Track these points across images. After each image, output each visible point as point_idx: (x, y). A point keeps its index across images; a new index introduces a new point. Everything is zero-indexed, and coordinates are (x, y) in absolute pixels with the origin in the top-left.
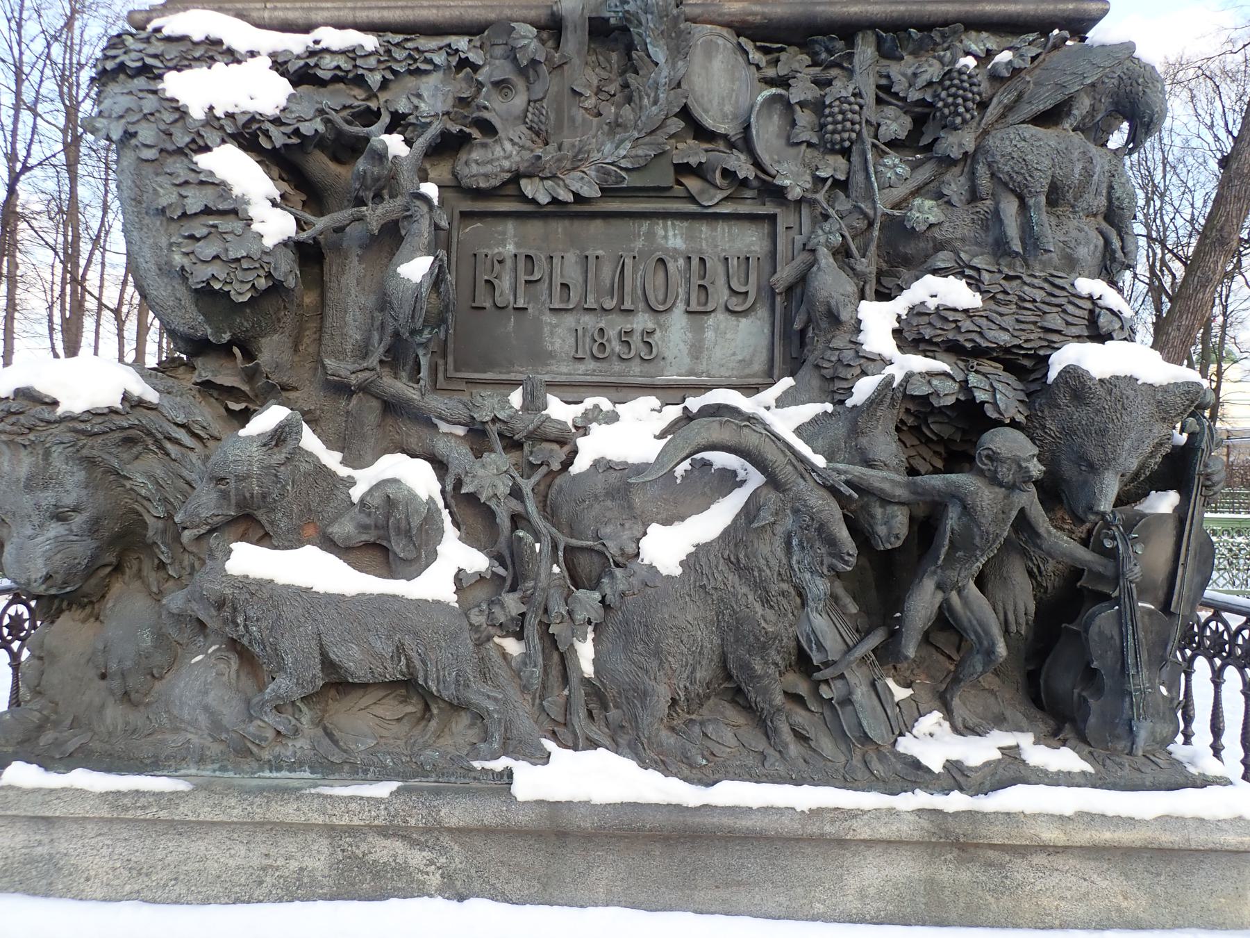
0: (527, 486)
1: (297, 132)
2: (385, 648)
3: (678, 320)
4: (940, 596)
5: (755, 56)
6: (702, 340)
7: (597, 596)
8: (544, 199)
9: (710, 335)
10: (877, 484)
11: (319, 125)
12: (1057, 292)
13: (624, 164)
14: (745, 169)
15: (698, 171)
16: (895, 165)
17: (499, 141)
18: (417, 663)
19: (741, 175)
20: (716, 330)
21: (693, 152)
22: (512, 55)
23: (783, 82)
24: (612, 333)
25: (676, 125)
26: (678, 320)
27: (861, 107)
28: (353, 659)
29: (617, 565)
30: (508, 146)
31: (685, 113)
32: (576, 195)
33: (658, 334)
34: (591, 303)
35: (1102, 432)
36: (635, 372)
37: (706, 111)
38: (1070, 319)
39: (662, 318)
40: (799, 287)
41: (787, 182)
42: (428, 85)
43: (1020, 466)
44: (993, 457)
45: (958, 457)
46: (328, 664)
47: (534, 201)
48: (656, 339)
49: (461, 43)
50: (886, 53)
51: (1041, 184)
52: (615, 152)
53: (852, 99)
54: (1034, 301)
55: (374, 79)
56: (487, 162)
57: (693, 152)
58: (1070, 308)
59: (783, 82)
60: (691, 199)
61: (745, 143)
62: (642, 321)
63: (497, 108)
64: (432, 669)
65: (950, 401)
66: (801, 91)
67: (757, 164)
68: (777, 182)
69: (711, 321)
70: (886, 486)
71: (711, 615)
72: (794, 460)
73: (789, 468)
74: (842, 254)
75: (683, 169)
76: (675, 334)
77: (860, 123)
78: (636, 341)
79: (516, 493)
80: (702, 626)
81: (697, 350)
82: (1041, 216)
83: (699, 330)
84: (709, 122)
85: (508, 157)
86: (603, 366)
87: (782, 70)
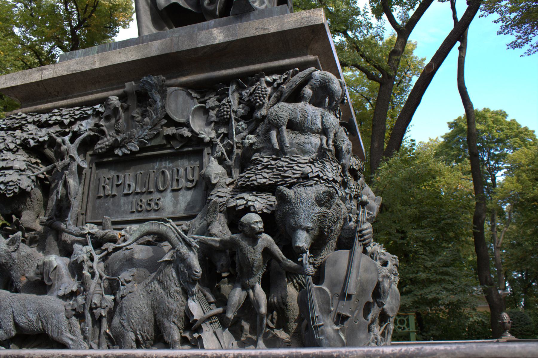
0: (96, 257)
1: (38, 140)
2: (33, 317)
3: (169, 195)
4: (245, 293)
5: (194, 94)
6: (177, 201)
7: (113, 297)
8: (120, 154)
9: (181, 198)
10: (209, 243)
11: (46, 138)
12: (292, 162)
13: (147, 137)
17: (106, 136)
18: (45, 324)
19: (185, 135)
20: (182, 196)
21: (171, 131)
24: (144, 200)
25: (165, 122)
26: (169, 195)
27: (230, 106)
28: (22, 321)
29: (123, 285)
30: (108, 137)
31: (167, 117)
32: (131, 151)
33: (162, 200)
34: (138, 190)
35: (294, 213)
36: (153, 216)
37: (176, 116)
38: (294, 172)
39: (163, 194)
41: (203, 136)
43: (250, 226)
44: (242, 225)
46: (17, 325)
47: (117, 155)
48: (160, 203)
50: (240, 88)
51: (285, 122)
53: (227, 104)
54: (283, 167)
55: (66, 122)
57: (171, 131)
58: (296, 168)
60: (172, 148)
61: (187, 125)
62: (156, 196)
64: (50, 327)
65: (242, 207)
67: (192, 131)
68: (199, 136)
69: (180, 193)
70: (213, 243)
71: (149, 302)
72: (178, 236)
73: (176, 238)
75: (169, 138)
77: (230, 112)
78: (153, 204)
79: (92, 259)
80: (146, 307)
81: (176, 203)
83: (176, 198)
84: (177, 119)
85: (108, 141)
86: (141, 214)
87: (206, 98)
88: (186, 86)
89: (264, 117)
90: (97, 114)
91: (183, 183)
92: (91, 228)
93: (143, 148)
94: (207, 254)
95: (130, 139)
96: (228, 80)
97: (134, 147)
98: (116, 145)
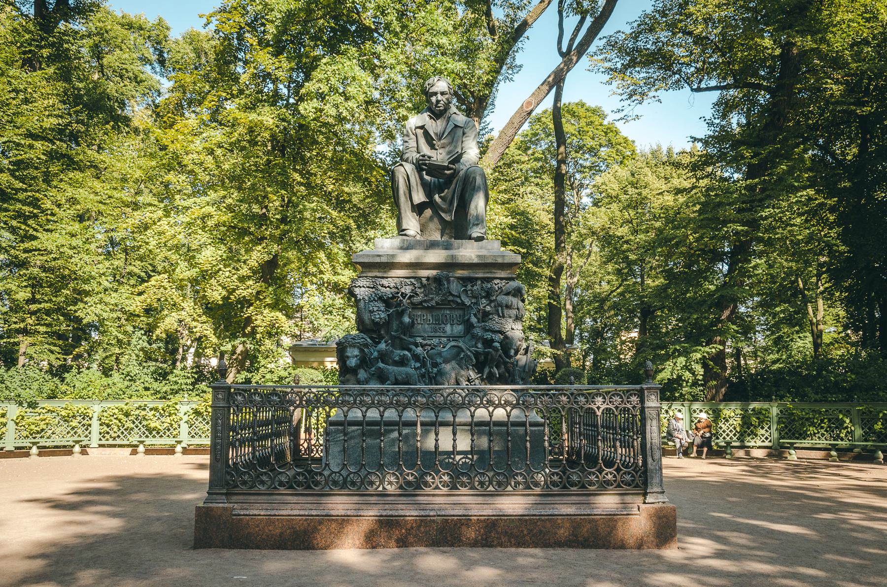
3: (449, 325)
14: (459, 301)
15: (452, 301)
16: (484, 301)
21: (451, 298)
22: (421, 283)
23: (465, 286)
26: (449, 325)
28: (400, 378)
36: (442, 334)
40: (469, 319)
42: (407, 287)
45: (491, 346)
46: (396, 379)
49: (413, 280)
50: (482, 282)
52: (437, 298)
56: (416, 300)
57: (451, 298)
59: (465, 286)
61: (459, 297)
62: (443, 326)
63: (419, 291)
66: (469, 287)
74: (475, 315)
75: (449, 301)
76: (448, 328)
81: (452, 330)
82: (505, 311)
88: (459, 278)
89: (494, 301)
90: (413, 284)
91: (455, 321)
92: (419, 340)
93: (437, 303)
94: (477, 354)
95: (432, 299)
96: (477, 279)
97: (433, 303)
98: (425, 301)
